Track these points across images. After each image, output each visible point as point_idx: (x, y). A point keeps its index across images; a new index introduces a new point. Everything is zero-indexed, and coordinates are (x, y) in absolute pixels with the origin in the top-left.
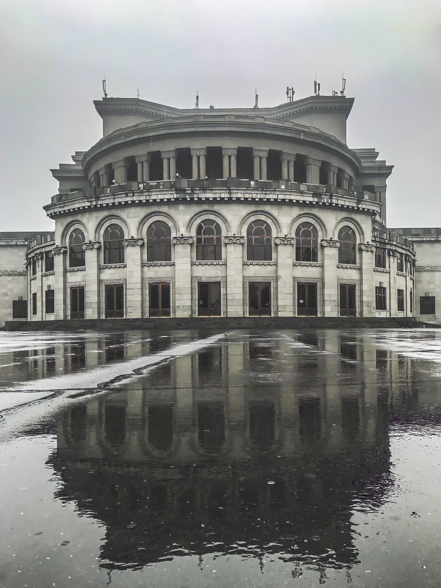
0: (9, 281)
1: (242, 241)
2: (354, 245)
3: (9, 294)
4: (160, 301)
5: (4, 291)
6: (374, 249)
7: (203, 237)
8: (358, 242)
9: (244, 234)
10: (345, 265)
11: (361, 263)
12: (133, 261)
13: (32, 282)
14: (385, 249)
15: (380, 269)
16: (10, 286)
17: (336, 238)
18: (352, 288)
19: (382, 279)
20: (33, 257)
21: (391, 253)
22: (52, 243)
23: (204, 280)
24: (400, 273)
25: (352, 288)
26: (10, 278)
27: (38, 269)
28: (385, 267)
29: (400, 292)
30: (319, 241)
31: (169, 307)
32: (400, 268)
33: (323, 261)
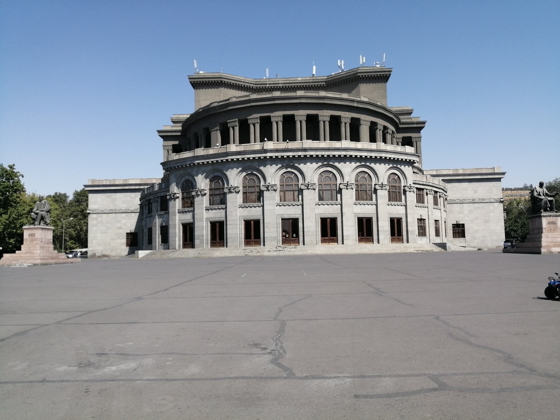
0: (124, 218)
1: (314, 187)
2: (400, 187)
3: (123, 227)
4: (253, 233)
5: (119, 225)
6: (415, 190)
7: (285, 184)
8: (403, 185)
9: (316, 181)
10: (393, 203)
11: (406, 201)
12: (232, 203)
13: (148, 219)
14: (423, 189)
15: (420, 205)
16: (124, 221)
17: (385, 182)
18: (399, 220)
19: (422, 213)
20: (149, 200)
21: (428, 193)
22: (167, 189)
23: (286, 217)
24: (436, 207)
25: (399, 220)
26: (124, 215)
27: (154, 209)
28: (423, 203)
29: (436, 221)
30: (373, 186)
31: (259, 238)
32: (436, 203)
33: (377, 200)
